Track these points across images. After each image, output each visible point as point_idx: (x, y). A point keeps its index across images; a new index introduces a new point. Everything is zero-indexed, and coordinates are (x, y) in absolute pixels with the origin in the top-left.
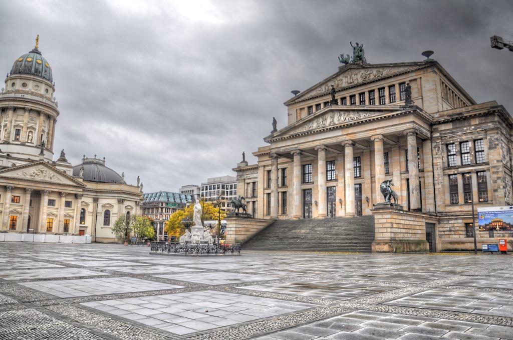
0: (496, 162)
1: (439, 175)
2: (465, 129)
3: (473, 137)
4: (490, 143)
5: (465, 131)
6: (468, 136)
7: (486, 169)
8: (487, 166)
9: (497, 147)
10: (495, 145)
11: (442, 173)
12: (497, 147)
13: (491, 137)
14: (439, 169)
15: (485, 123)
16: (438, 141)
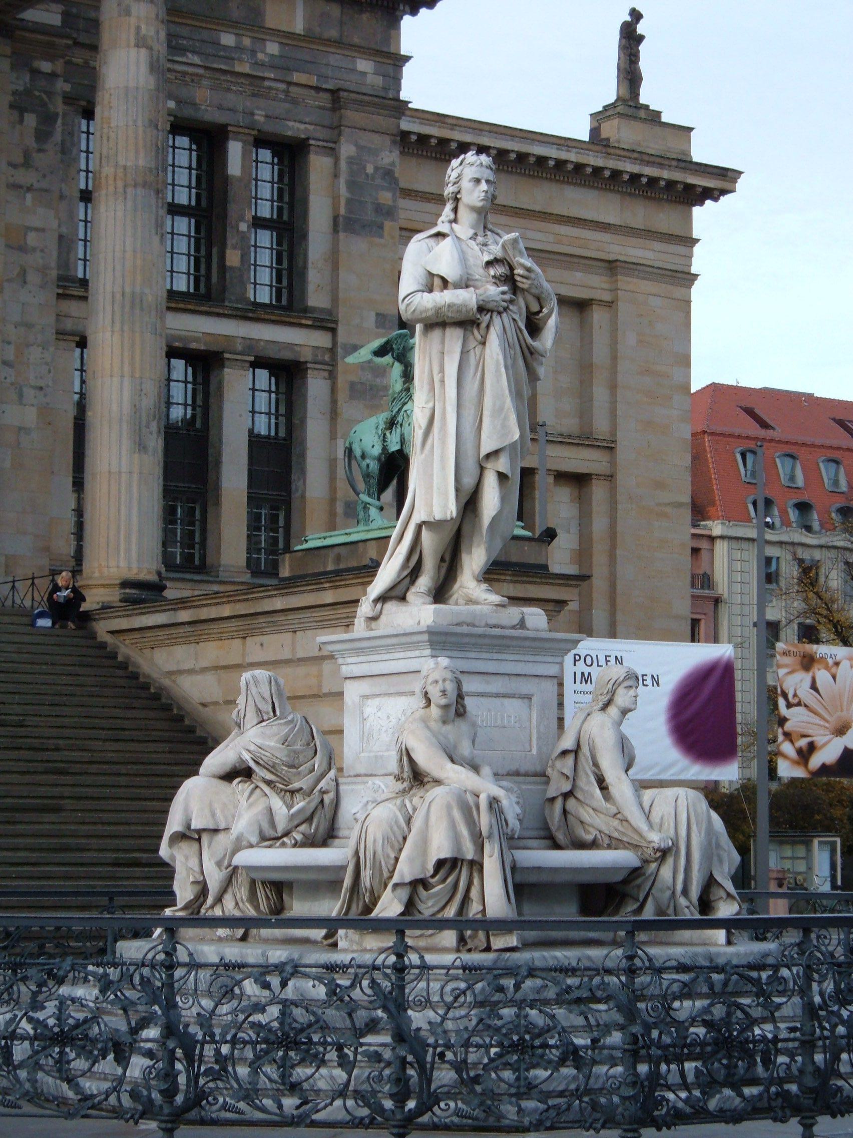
0: (372, 318)
1: (29, 326)
2: (227, 39)
3: (259, 117)
4: (352, 185)
5: (229, 55)
6: (231, 99)
7: (306, 355)
8: (320, 339)
9: (388, 224)
10: (379, 209)
11: (49, 320)
12: (388, 224)
13: (359, 148)
14: (33, 278)
15: (338, 43)
16: (46, 66)
